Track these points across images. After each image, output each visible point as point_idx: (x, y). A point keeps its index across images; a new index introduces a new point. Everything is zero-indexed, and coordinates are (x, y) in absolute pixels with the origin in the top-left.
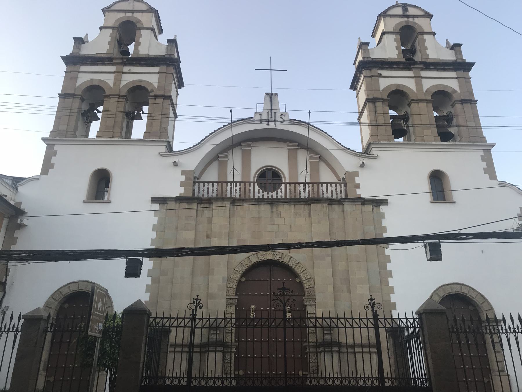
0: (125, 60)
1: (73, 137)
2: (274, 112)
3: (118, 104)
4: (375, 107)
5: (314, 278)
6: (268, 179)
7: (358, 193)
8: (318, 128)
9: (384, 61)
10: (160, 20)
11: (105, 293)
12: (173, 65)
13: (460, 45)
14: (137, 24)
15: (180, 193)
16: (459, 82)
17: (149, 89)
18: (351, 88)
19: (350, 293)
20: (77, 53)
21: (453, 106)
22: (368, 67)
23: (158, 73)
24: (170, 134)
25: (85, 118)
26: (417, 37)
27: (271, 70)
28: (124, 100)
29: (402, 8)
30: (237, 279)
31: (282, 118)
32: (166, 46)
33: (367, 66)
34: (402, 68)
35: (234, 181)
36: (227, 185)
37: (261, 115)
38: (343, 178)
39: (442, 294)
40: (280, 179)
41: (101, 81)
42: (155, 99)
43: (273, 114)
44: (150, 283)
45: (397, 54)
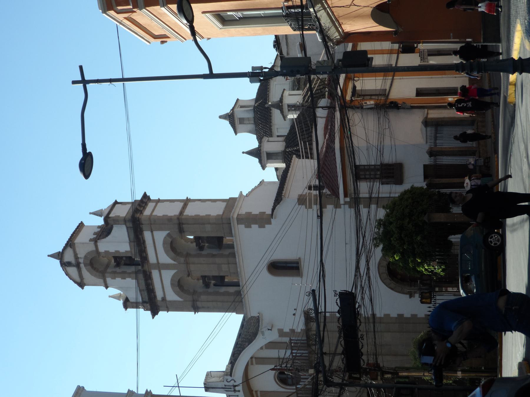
4: (203, 307)
27: (179, 387)
29: (67, 267)
34: (151, 281)
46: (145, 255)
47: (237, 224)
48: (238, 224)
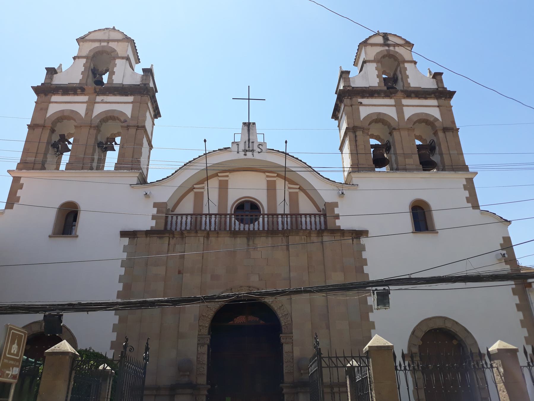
0: (98, 90)
1: (41, 169)
2: (252, 142)
3: (89, 135)
4: (356, 136)
5: (292, 316)
6: (246, 211)
7: (337, 224)
8: (297, 159)
9: (365, 89)
10: (136, 50)
11: (23, 334)
12: (147, 94)
13: (441, 74)
14: (112, 54)
15: (151, 227)
16: (440, 111)
17: (122, 119)
18: (332, 118)
19: (329, 330)
20: (48, 83)
21: (435, 133)
22: (348, 96)
23: (132, 103)
24: (143, 166)
25: (56, 150)
26: (399, 65)
27: (249, 99)
28: (95, 131)
30: (210, 317)
31: (259, 148)
32: (141, 76)
33: (347, 95)
34: (383, 97)
35: (210, 213)
36: (201, 218)
37: (238, 145)
38: (323, 209)
39: (426, 329)
40: (259, 211)
41: (72, 111)
42: (128, 129)
43: (251, 144)
44: (117, 322)
45: (378, 83)
46: (413, 96)
47: (467, 177)
48: (466, 179)
